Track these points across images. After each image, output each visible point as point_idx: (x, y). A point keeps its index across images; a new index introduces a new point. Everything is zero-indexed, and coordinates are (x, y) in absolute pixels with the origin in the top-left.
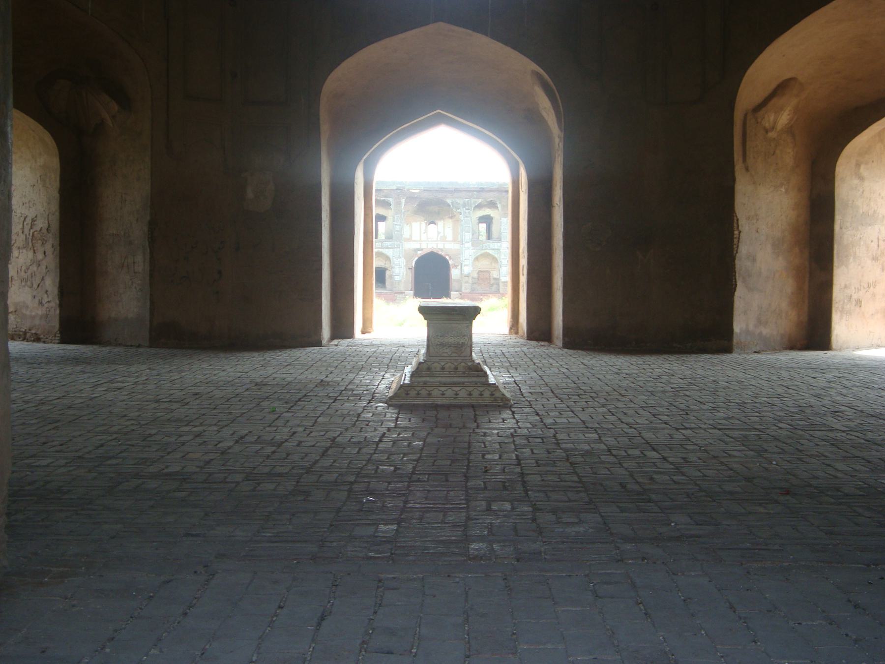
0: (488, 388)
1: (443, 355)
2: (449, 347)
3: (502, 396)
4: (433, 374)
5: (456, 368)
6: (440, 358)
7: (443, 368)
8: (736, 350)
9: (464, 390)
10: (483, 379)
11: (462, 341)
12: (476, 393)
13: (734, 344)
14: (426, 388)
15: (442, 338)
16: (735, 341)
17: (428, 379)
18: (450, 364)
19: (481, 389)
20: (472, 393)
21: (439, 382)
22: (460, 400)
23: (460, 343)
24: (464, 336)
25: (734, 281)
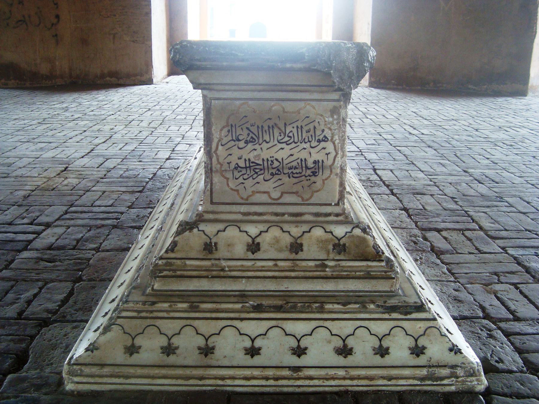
0: (405, 324)
1: (253, 199)
2: (272, 174)
3: (451, 359)
4: (223, 270)
6: (244, 209)
8: (530, 94)
9: (322, 333)
10: (382, 286)
11: (316, 156)
13: (529, 87)
14: (196, 323)
16: (530, 85)
17: (205, 285)
18: (275, 232)
19: (380, 328)
20: (350, 342)
21: (243, 296)
22: (311, 378)
23: (310, 164)
24: (325, 139)
25: (535, 28)
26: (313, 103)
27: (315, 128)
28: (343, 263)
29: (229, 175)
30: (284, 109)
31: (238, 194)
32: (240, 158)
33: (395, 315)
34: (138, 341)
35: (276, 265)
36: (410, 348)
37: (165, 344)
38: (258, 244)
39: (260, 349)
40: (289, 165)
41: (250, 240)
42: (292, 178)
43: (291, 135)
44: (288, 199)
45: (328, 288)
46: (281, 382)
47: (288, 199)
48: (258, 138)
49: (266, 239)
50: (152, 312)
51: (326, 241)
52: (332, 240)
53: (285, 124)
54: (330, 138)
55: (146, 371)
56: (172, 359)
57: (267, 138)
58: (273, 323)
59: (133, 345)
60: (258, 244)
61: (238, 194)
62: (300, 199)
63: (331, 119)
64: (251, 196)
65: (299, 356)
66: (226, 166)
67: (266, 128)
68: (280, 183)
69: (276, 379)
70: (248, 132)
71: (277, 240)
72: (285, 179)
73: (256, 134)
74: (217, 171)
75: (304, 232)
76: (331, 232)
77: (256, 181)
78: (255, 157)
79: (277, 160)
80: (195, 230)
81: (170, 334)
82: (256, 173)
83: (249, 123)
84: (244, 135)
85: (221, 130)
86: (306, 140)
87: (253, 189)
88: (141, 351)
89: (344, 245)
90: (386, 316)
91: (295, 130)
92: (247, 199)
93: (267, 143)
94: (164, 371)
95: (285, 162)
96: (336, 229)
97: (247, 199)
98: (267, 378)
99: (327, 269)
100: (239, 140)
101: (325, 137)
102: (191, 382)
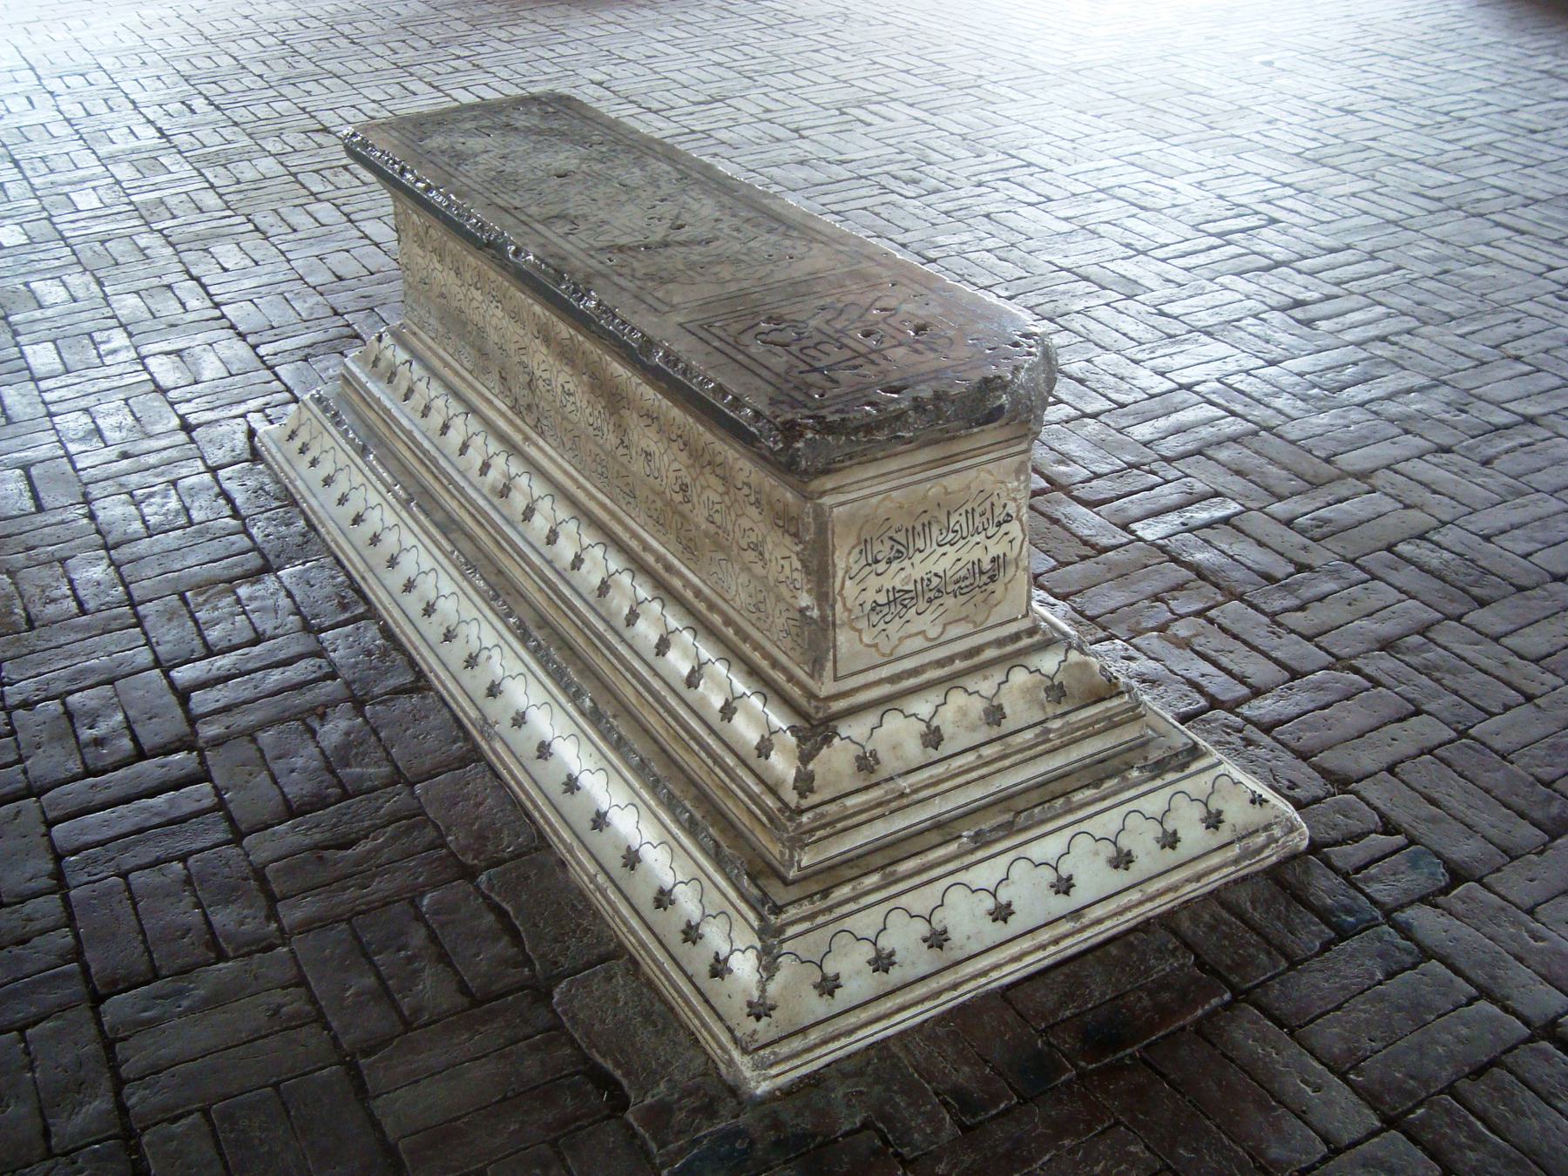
0: (1183, 785)
1: (902, 651)
2: (930, 601)
4: (902, 795)
5: (995, 714)
7: (933, 737)
10: (1129, 733)
11: (995, 550)
12: (1142, 841)
14: (903, 901)
15: (895, 565)
17: (880, 830)
19: (1154, 804)
20: (1125, 843)
22: (1099, 921)
23: (986, 565)
26: (990, 466)
27: (993, 504)
28: (1073, 718)
29: (863, 624)
30: (946, 488)
31: (878, 650)
32: (879, 591)
33: (1170, 777)
34: (830, 968)
35: (980, 756)
36: (1203, 821)
37: (872, 954)
38: (938, 728)
39: (1009, 905)
40: (955, 578)
41: (923, 727)
42: (960, 597)
43: (957, 527)
44: (954, 631)
45: (1057, 764)
46: (1063, 944)
47: (954, 631)
48: (908, 549)
49: (947, 720)
50: (830, 909)
51: (1036, 686)
52: (1042, 682)
53: (949, 513)
54: (1014, 515)
55: (873, 1011)
56: (896, 976)
57: (920, 544)
58: (1012, 855)
59: (824, 978)
60: (938, 728)
61: (878, 650)
62: (971, 626)
63: (1016, 484)
64: (897, 646)
65: (1067, 893)
66: (857, 612)
67: (919, 528)
68: (941, 609)
69: (1056, 942)
70: (892, 543)
71: (963, 712)
72: (949, 601)
73: (904, 542)
74: (843, 624)
75: (999, 684)
76: (1038, 670)
77: (904, 620)
78: (906, 580)
79: (936, 575)
80: (836, 740)
81: (871, 934)
82: (905, 606)
83: (893, 530)
84: (884, 550)
85: (850, 553)
86: (980, 529)
87: (901, 634)
88: (842, 981)
89: (1061, 683)
90: (1158, 782)
91: (963, 519)
92: (891, 654)
93: (921, 552)
94: (899, 1000)
95: (949, 574)
96: (1043, 663)
97: (891, 654)
98: (1043, 947)
99: (1051, 736)
100: (877, 561)
101: (1008, 515)
102: (944, 998)
